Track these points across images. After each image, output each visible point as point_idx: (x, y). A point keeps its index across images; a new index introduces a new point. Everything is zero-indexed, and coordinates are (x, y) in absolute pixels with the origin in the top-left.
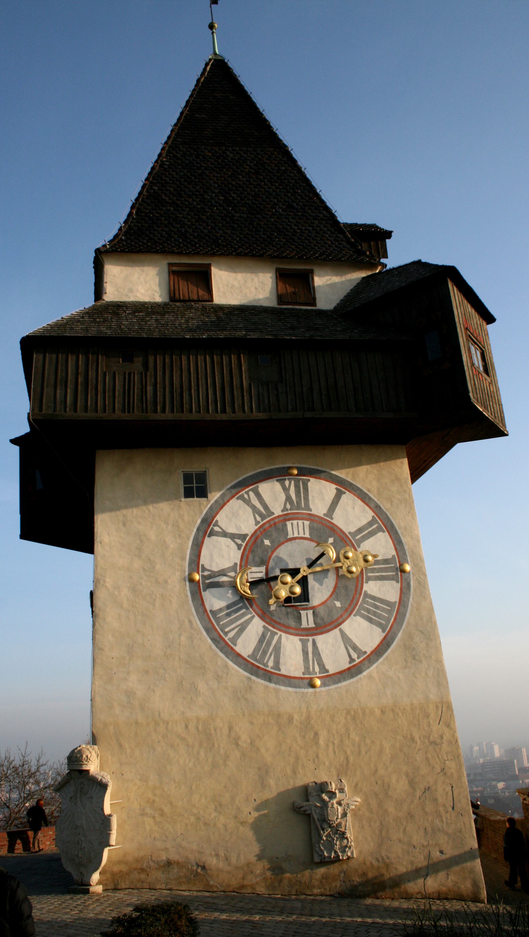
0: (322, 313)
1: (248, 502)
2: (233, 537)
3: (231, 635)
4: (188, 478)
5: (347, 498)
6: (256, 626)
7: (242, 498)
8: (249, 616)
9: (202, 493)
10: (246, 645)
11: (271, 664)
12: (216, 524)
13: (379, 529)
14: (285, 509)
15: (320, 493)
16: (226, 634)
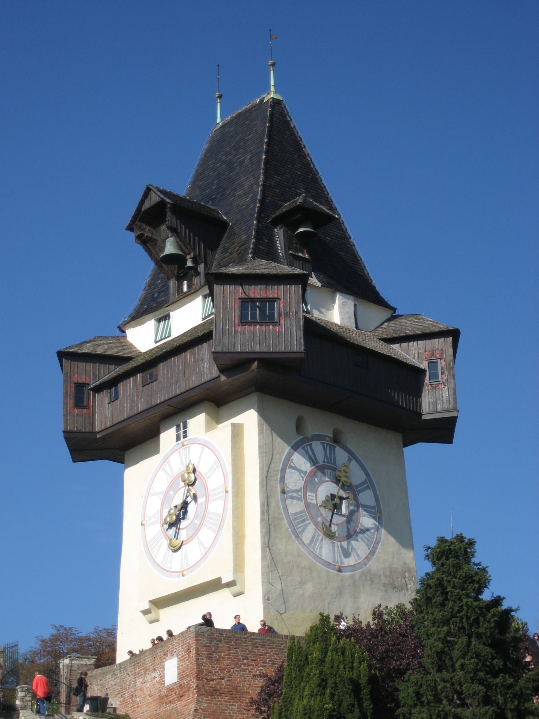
2: (300, 471)
3: (300, 530)
5: (354, 463)
7: (303, 448)
8: (308, 522)
11: (318, 551)
12: (292, 462)
13: (367, 488)
14: (324, 462)
16: (298, 528)
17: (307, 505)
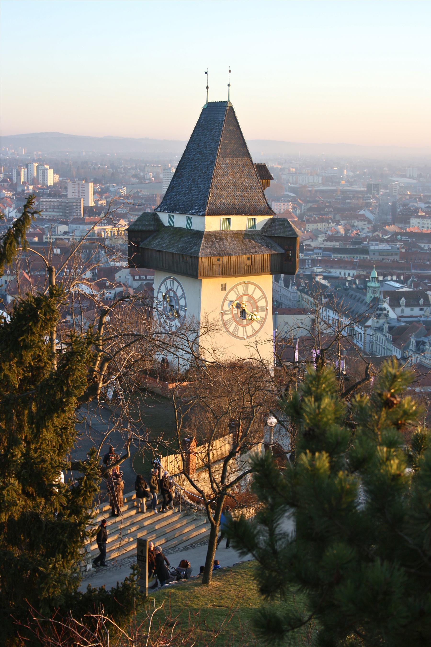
0: (257, 232)
1: (235, 292)
4: (222, 285)
5: (257, 289)
6: (234, 324)
9: (225, 289)
10: (231, 330)
15: (251, 288)
17: (233, 314)
